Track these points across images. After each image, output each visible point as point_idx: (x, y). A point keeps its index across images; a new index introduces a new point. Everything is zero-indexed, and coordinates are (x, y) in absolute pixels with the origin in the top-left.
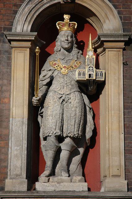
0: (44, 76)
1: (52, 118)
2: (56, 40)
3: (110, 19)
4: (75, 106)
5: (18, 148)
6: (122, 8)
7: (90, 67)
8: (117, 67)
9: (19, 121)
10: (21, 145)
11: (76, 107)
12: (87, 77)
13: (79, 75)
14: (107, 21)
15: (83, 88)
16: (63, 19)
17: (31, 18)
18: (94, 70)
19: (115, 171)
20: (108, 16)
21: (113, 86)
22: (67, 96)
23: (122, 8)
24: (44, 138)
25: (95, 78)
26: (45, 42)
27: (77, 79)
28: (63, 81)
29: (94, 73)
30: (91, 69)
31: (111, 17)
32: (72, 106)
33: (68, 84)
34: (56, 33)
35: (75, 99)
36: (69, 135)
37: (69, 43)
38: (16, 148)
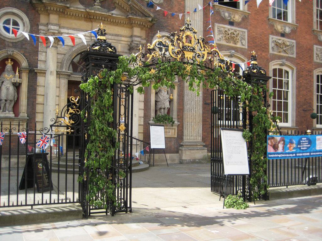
14: (23, 63)
19: (24, 111)
31: (25, 62)
34: (5, 65)
35: (11, 88)
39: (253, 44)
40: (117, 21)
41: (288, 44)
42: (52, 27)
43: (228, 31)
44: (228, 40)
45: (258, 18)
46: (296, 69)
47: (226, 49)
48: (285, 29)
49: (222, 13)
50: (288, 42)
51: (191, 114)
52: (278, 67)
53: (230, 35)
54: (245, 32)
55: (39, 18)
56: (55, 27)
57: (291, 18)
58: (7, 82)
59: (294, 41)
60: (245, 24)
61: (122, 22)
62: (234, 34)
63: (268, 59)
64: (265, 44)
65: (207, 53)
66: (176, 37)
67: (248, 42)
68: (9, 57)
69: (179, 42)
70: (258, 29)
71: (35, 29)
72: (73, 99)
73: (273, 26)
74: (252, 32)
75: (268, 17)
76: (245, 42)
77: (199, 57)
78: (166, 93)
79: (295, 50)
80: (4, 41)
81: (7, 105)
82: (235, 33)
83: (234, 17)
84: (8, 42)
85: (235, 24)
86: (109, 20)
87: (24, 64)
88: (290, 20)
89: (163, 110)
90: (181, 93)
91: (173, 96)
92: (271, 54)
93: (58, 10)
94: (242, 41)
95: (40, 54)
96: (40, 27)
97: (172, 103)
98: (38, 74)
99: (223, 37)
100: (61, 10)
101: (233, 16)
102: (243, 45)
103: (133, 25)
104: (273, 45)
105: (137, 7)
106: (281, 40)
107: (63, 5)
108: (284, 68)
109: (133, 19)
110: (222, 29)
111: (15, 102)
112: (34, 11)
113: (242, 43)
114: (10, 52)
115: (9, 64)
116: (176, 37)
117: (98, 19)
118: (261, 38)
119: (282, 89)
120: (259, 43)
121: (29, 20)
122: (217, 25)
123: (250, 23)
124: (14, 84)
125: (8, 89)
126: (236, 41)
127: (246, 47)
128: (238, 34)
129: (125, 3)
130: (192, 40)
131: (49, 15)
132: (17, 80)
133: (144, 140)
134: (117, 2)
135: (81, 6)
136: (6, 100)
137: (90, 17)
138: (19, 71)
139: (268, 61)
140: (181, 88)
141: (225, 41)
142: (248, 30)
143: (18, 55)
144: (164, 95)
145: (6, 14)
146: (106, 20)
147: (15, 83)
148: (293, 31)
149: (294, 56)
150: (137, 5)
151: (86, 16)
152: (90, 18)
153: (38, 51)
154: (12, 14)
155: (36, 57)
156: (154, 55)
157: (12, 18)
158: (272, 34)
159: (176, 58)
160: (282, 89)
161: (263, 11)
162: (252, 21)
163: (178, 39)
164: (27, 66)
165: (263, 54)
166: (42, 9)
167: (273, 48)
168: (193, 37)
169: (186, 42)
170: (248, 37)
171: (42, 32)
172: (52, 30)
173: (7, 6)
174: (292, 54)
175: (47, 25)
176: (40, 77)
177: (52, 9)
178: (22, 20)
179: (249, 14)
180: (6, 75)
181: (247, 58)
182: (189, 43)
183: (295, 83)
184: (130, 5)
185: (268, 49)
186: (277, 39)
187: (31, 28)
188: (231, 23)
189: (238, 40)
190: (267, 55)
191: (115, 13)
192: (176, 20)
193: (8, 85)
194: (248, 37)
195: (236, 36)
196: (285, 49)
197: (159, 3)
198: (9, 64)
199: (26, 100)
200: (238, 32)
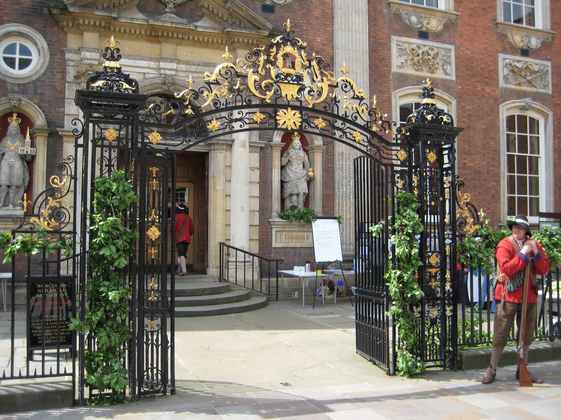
8: (43, 147)
12: (25, 153)
16: (12, 116)
31: (40, 118)
34: (8, 124)
35: (18, 165)
39: (466, 72)
40: (206, 39)
41: (536, 68)
42: (88, 55)
43: (417, 49)
44: (417, 66)
45: (475, 22)
46: (553, 116)
47: (415, 83)
48: (529, 42)
49: (405, 17)
50: (536, 64)
51: (348, 204)
52: (516, 113)
53: (421, 56)
54: (450, 50)
55: (66, 39)
56: (94, 54)
57: (541, 22)
58: (10, 153)
59: (549, 64)
60: (451, 35)
61: (215, 41)
62: (428, 53)
63: (496, 99)
64: (491, 71)
65: (329, 85)
66: (262, 58)
67: (457, 69)
68: (15, 110)
69: (268, 66)
70: (477, 44)
71: (59, 59)
72: (56, 181)
73: (505, 36)
74: (464, 49)
75: (495, 20)
76: (452, 69)
77: (312, 93)
78: (301, 166)
79: (550, 80)
80: (5, 82)
81: (12, 195)
82: (430, 52)
83: (428, 23)
84: (11, 83)
85: (430, 36)
86: (191, 38)
87: (40, 121)
88: (539, 24)
89: (295, 198)
90: (330, 165)
91: (313, 171)
92: (501, 88)
93: (98, 24)
94: (445, 67)
95: (68, 103)
96: (68, 56)
97: (312, 184)
98: (65, 139)
99: (409, 61)
100: (103, 24)
101: (427, 21)
102: (446, 74)
103: (235, 45)
104: (506, 71)
105: (240, 13)
106: (521, 61)
107: (105, 15)
108: (530, 114)
109: (235, 34)
110: (406, 45)
112: (56, 29)
113: (444, 70)
114: (15, 102)
115: (14, 123)
116: (262, 58)
117: (170, 37)
118: (482, 59)
119: (527, 153)
120: (479, 69)
121: (48, 44)
122: (395, 39)
123: (459, 34)
124: (23, 158)
125: (11, 167)
126: (434, 67)
127: (454, 78)
128: (437, 53)
129: (220, 7)
130: (296, 61)
131: (82, 34)
132: (27, 149)
133: (261, 252)
134: (206, 5)
135: (140, 16)
136: (9, 187)
137: (156, 34)
138: (30, 134)
139: (497, 101)
140: (329, 157)
141: (412, 67)
142: (456, 46)
143: (30, 105)
144: (296, 172)
145: (8, 35)
146: (186, 38)
147: (25, 156)
148: (546, 45)
149: (549, 91)
150: (241, 9)
151: (148, 33)
152: (157, 36)
153: (64, 98)
154: (18, 35)
155: (61, 108)
156: (218, 93)
157: (18, 41)
158: (504, 51)
159: (264, 97)
160: (527, 153)
161: (484, 9)
162: (463, 29)
163: (267, 61)
164: (45, 126)
165: (488, 89)
166: (70, 24)
167: (506, 78)
168: (297, 55)
169: (284, 66)
170: (456, 59)
171: (71, 63)
172: (87, 59)
173: (9, 22)
174: (545, 87)
175: (79, 51)
176: (67, 144)
177: (87, 22)
178: (36, 44)
179: (457, 15)
180: (9, 142)
181: (456, 98)
182: (289, 67)
183: (551, 141)
184: (228, 10)
185: (496, 80)
186: (514, 61)
187: (50, 58)
188: (423, 35)
189: (437, 66)
190: (495, 91)
191: (204, 25)
192: (317, 33)
193: (12, 160)
194: (457, 58)
195: (433, 58)
196: (529, 78)
197: (286, 3)
198: (14, 123)
199: (43, 184)
200: (436, 51)
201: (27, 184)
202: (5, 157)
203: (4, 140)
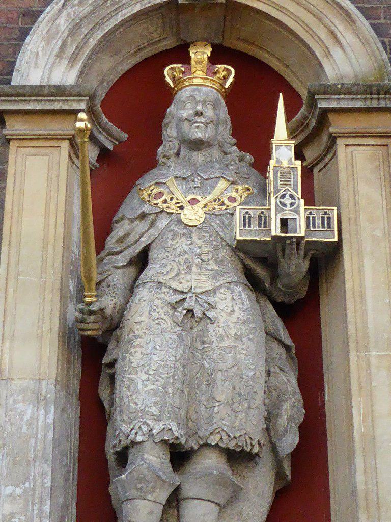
0: (121, 240)
1: (145, 377)
2: (165, 121)
3: (345, 44)
4: (233, 332)
5: (19, 491)
6: (382, 16)
7: (283, 196)
9: (24, 390)
10: (27, 479)
11: (238, 338)
12: (275, 230)
13: (245, 226)
14: (337, 53)
15: (261, 272)
17: (79, 49)
18: (299, 206)
20: (339, 36)
21: (368, 264)
22: (203, 297)
23: (382, 16)
24: (116, 453)
25: (303, 234)
26: (127, 135)
27: (238, 238)
28: (186, 248)
29: (299, 214)
30: (288, 201)
32: (221, 332)
33: (205, 258)
35: (235, 313)
36: (213, 441)
37: (206, 124)
38: (9, 490)
111: (279, 475)
125: (191, 316)
132: (286, 211)
201: (290, 441)
202: (148, 274)
203: (147, 186)
